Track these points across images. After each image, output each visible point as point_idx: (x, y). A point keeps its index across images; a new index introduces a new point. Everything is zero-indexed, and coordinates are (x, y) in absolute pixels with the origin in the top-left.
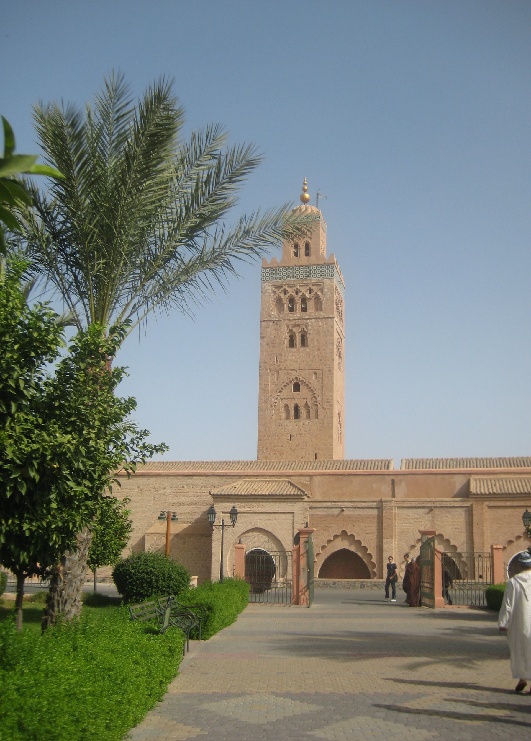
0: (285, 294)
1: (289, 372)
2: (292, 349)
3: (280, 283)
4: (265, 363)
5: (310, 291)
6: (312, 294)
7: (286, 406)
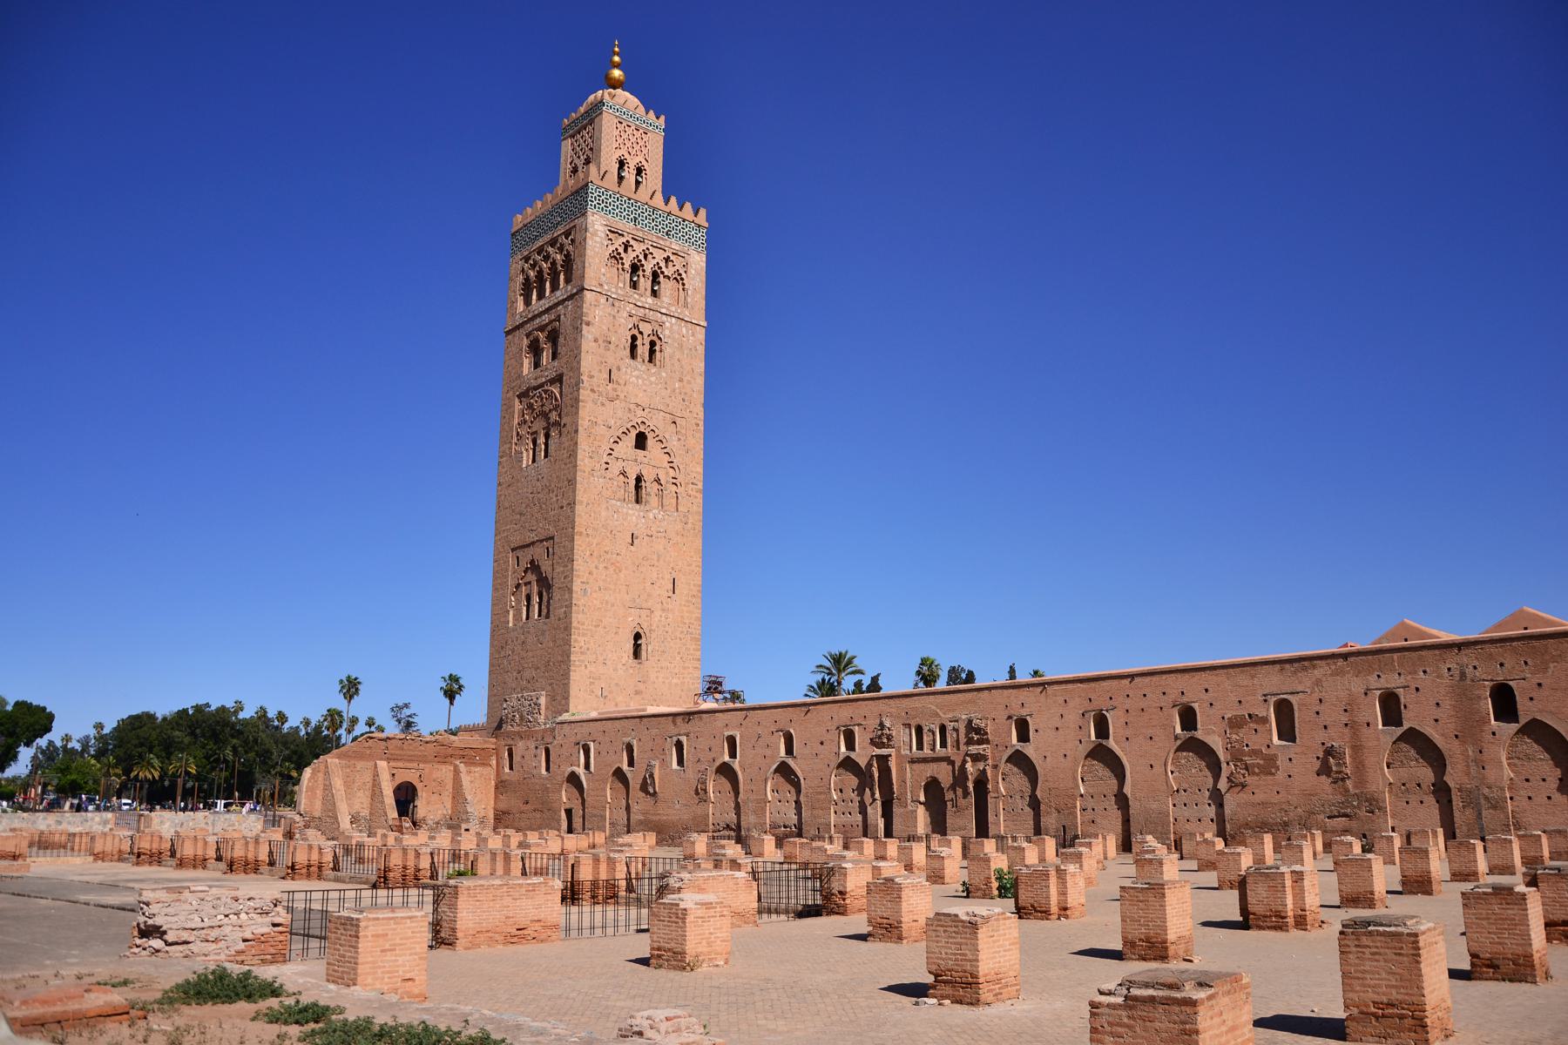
0: (626, 251)
5: (667, 260)
7: (623, 473)
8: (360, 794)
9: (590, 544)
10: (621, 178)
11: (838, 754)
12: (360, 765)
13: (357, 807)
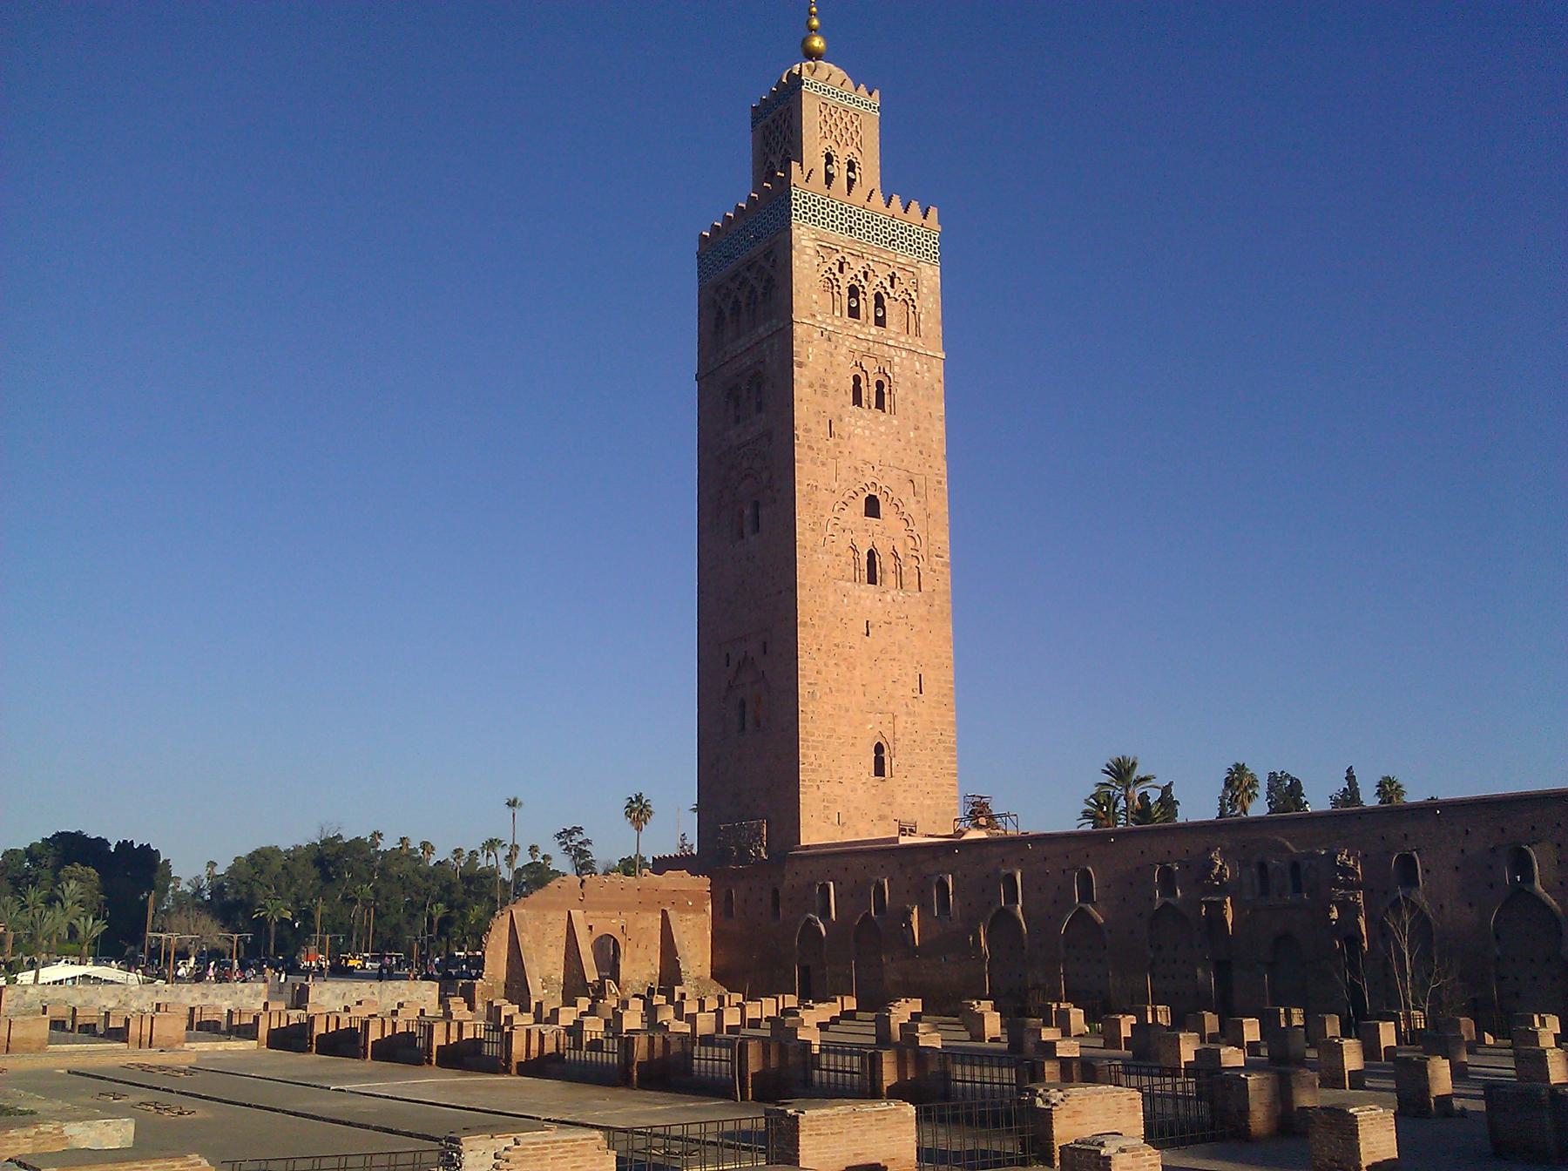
0: (841, 270)
1: (860, 465)
4: (808, 431)
8: (552, 951)
9: (816, 636)
10: (829, 178)
11: (1152, 899)
13: (549, 967)
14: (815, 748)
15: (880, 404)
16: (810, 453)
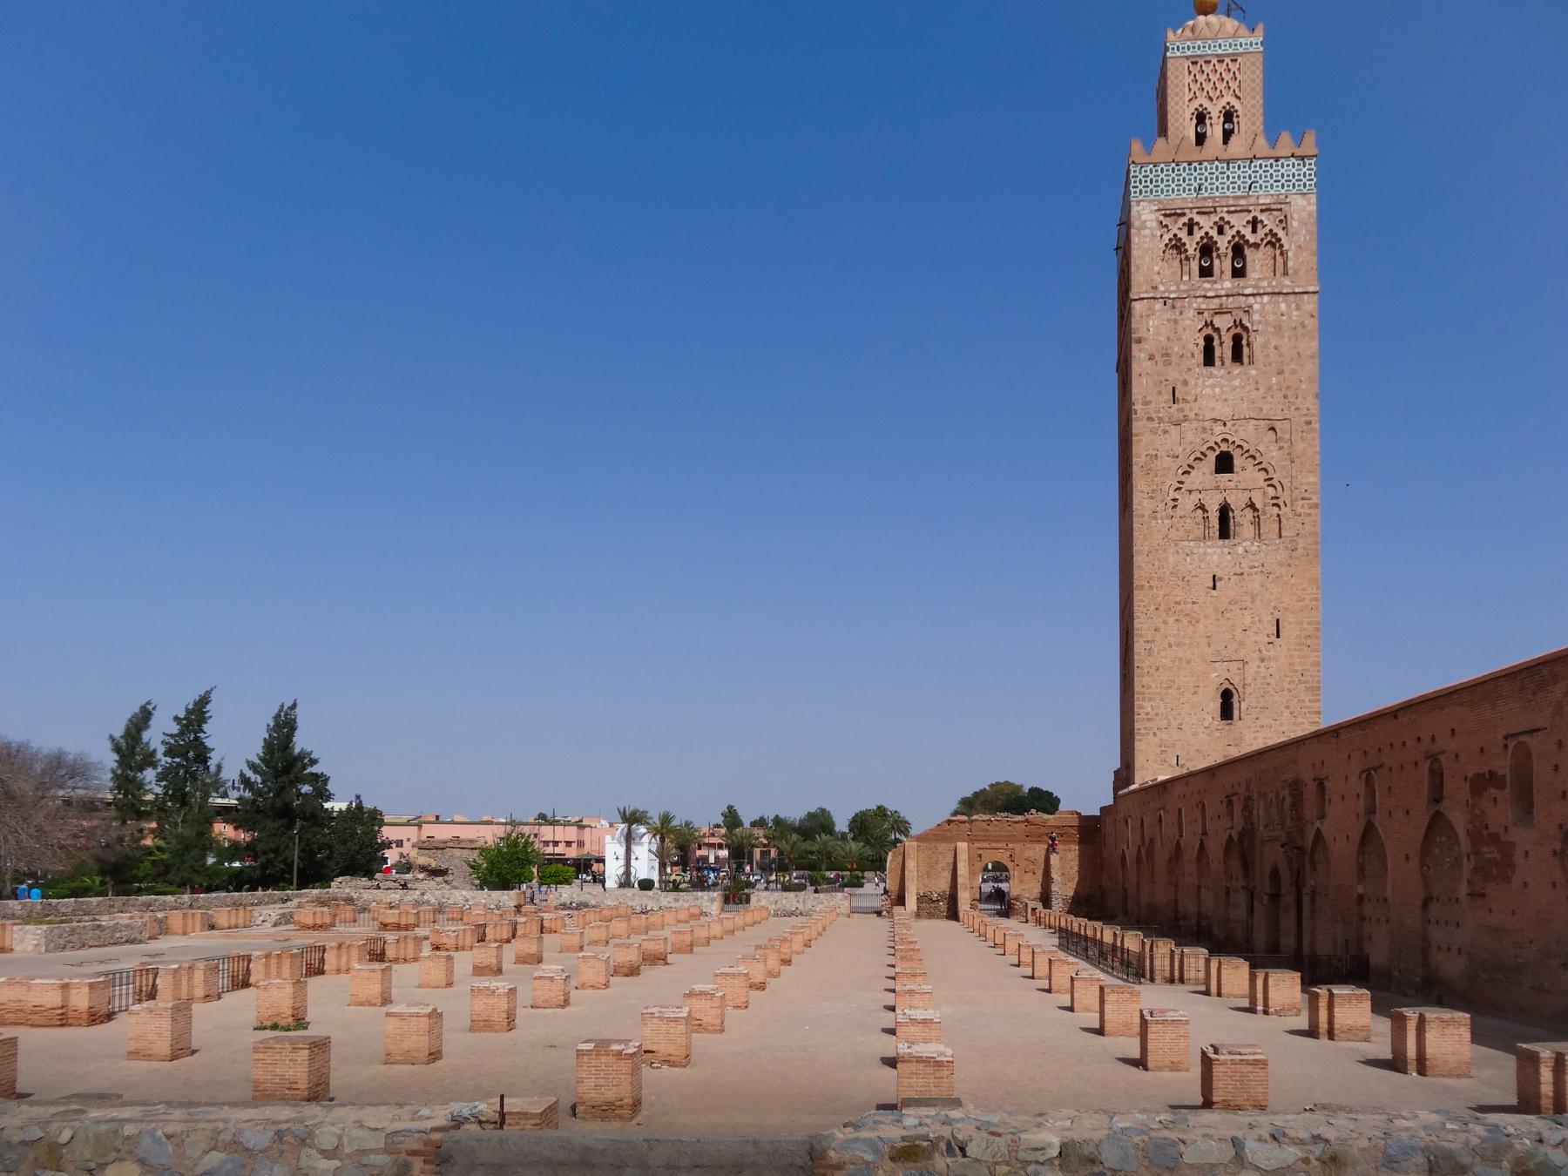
0: (1190, 233)
1: (1207, 424)
2: (1211, 369)
3: (1179, 204)
4: (1147, 403)
5: (1254, 224)
6: (1261, 232)
7: (1202, 507)
12: (942, 847)
14: (1150, 700)
15: (1237, 356)
16: (1150, 425)
